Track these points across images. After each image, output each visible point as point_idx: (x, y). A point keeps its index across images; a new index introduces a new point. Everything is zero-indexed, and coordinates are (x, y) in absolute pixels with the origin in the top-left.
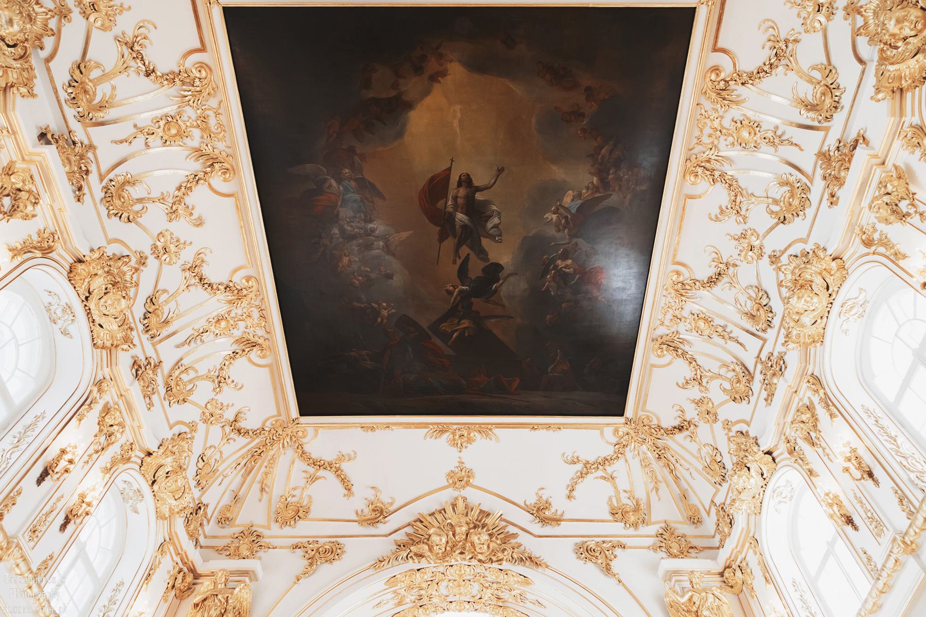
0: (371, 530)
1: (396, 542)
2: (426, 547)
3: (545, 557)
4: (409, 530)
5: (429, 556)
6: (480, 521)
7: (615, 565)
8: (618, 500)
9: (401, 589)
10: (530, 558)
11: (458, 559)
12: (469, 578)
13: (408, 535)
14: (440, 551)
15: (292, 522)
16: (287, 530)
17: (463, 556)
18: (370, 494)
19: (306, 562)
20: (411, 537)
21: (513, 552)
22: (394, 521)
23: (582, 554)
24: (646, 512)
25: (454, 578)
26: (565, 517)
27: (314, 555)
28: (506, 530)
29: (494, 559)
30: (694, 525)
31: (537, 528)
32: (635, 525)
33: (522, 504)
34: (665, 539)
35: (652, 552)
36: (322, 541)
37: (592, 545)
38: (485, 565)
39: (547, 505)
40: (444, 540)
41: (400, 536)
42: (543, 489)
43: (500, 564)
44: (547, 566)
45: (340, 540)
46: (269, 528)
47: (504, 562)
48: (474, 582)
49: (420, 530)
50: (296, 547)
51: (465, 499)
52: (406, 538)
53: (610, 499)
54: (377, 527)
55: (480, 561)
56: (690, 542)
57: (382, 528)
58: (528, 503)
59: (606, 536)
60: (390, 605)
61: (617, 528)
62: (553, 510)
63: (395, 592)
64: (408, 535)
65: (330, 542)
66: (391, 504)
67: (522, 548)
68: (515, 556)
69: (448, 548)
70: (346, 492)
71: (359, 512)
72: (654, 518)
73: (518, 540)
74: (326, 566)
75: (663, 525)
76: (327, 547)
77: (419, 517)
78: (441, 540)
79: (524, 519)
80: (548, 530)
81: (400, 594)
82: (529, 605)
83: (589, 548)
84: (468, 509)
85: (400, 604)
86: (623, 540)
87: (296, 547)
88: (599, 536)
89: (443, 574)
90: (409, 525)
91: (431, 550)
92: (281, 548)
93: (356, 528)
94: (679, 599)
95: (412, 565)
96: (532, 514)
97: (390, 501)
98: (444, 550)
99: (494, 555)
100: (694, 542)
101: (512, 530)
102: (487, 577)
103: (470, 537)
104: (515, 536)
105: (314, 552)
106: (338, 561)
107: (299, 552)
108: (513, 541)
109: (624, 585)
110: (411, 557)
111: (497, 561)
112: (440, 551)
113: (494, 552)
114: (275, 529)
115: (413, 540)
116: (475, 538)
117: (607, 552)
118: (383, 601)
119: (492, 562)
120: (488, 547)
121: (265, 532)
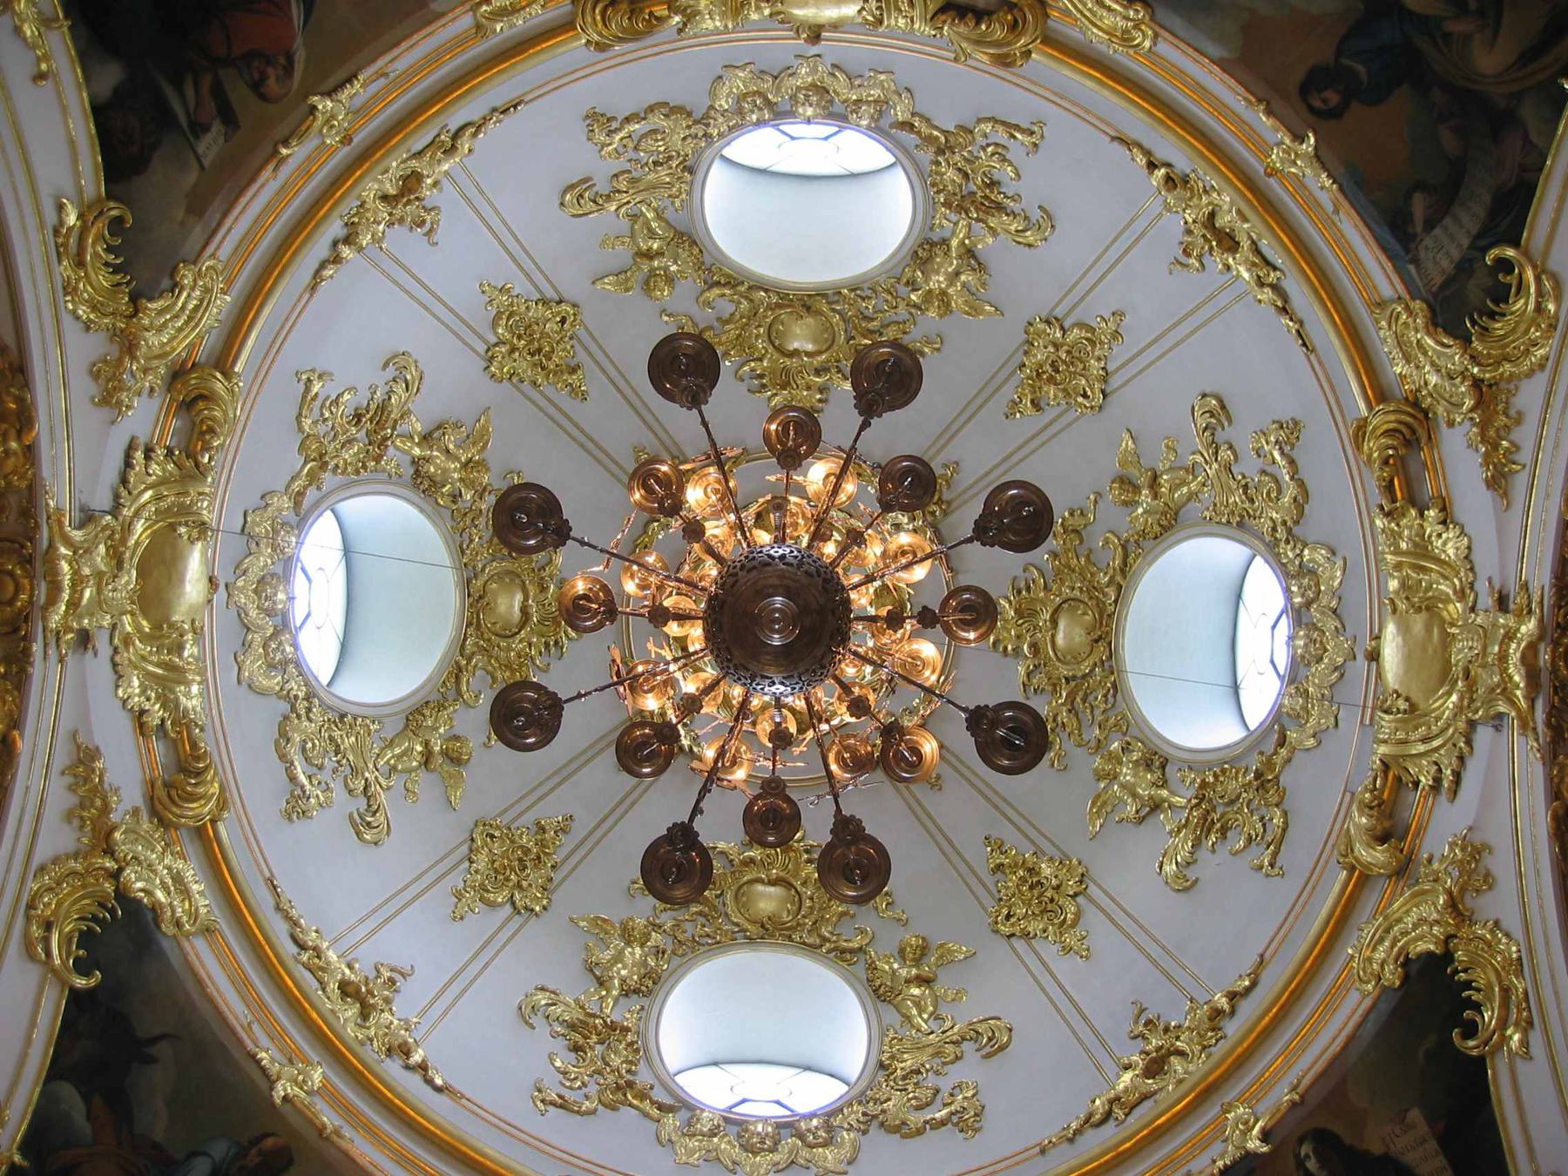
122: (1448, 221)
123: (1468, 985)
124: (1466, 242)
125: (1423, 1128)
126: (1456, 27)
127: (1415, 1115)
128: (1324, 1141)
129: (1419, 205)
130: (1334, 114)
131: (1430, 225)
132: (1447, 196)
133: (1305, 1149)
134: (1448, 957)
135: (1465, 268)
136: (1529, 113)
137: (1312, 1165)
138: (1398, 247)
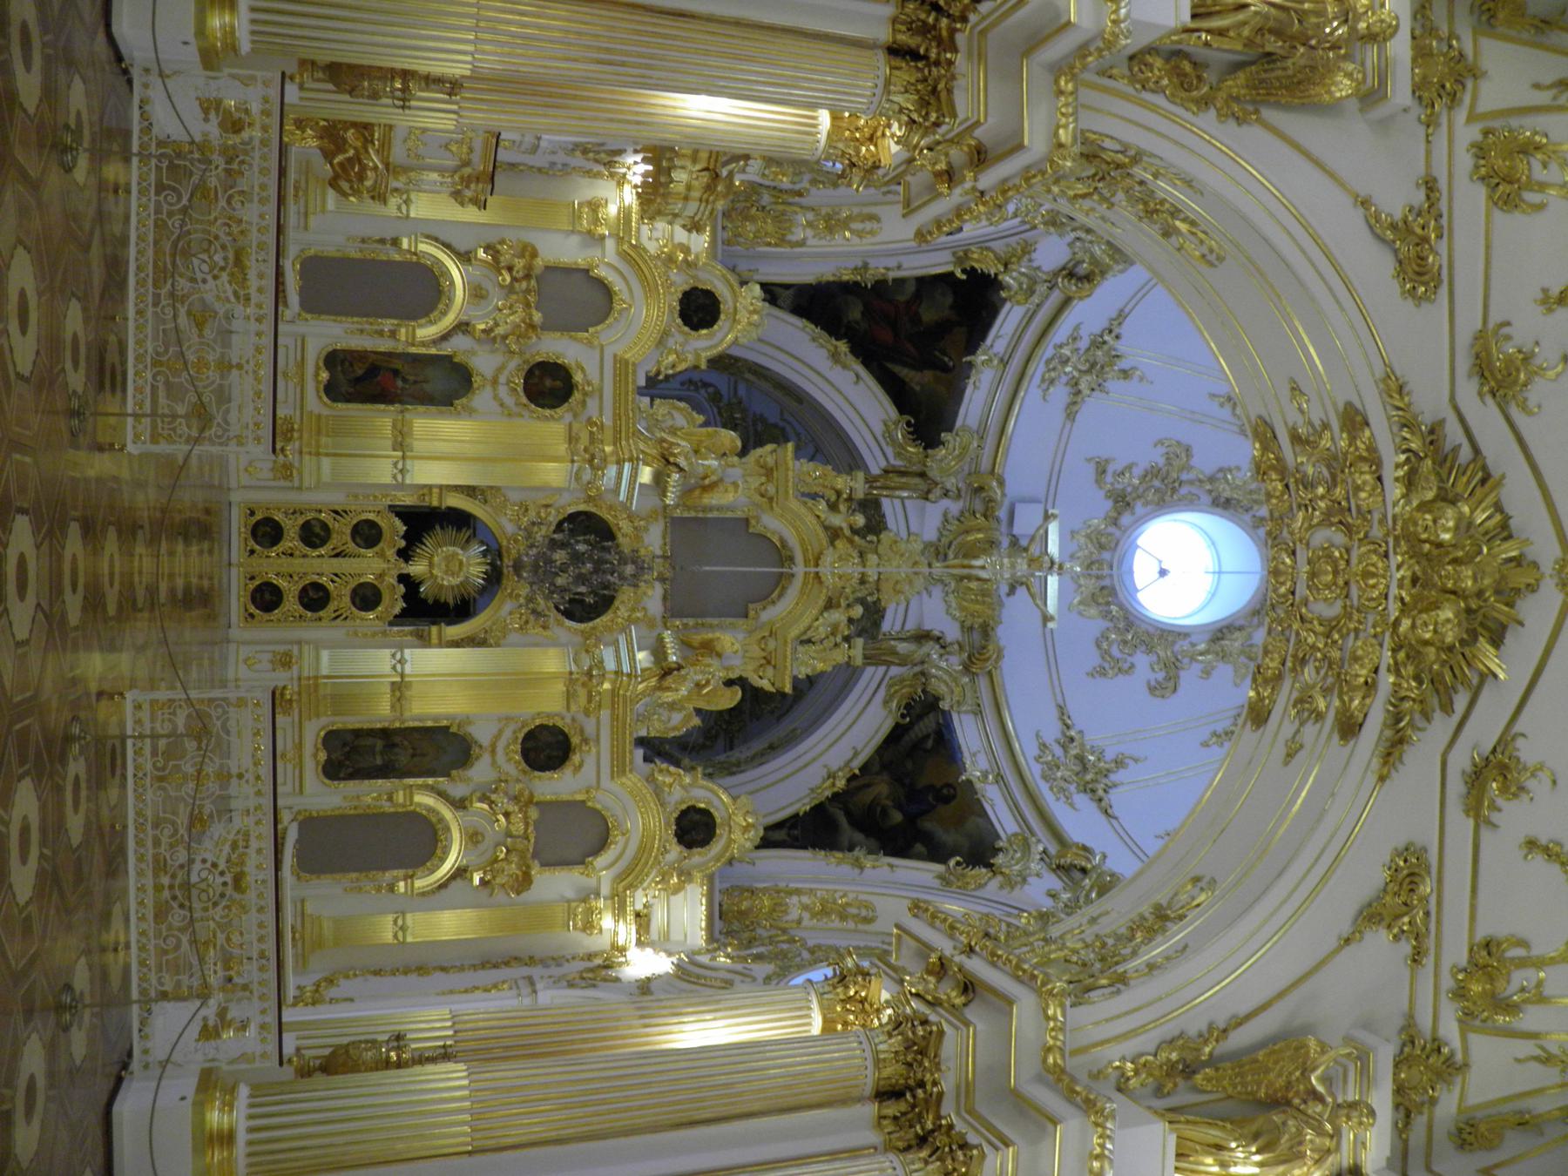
0: (1464, 364)
1: (1442, 422)
2: (1430, 495)
3: (1399, 778)
4: (1466, 453)
5: (1408, 502)
6: (1482, 624)
7: (1379, 939)
8: (1522, 963)
9: (1333, 439)
10: (1401, 741)
11: (1402, 572)
12: (1354, 592)
13: (1456, 449)
14: (1420, 529)
15: (1483, 171)
16: (1465, 161)
17: (1407, 582)
18: (1547, 355)
19: (1398, 216)
20: (1450, 457)
21: (1414, 700)
22: (1486, 419)
23: (1406, 861)
24: (1490, 1023)
25: (1354, 560)
26: (1486, 834)
27: (1413, 233)
28: (1460, 687)
29: (1401, 655)
30: (1453, 1130)
31: (1461, 760)
32: (1460, 993)
33: (1519, 727)
34: (1428, 1057)
35: (1399, 1022)
36: (1443, 247)
37: (1427, 888)
38: (1388, 635)
39: (1513, 789)
40: (1446, 536)
41: (1454, 434)
42: (1554, 782)
43: (1389, 670)
44: (1382, 779)
45: (1444, 291)
46: (1472, 118)
47: (1391, 679)
48: (1345, 607)
49: (1465, 479)
50: (1430, 185)
51: (1532, 588)
52: (1448, 447)
53: (1523, 943)
54: (1470, 376)
55: (1397, 623)
56: (1421, 1113)
57: (1468, 391)
58: (1520, 742)
59: (1439, 922)
60: (1294, 417)
61: (1456, 951)
62: (1500, 802)
63: (1326, 426)
64: (1456, 449)
65: (1440, 266)
66: (1524, 407)
67: (1420, 723)
68: (1407, 705)
69: (1427, 546)
70: (1555, 291)
71: (1506, 330)
72: (1475, 1039)
73: (1438, 715)
74: (1388, 264)
75: (1459, 1057)
76: (1431, 259)
77: (1496, 473)
78: (1447, 530)
79: (1484, 730)
80: (1456, 786)
81: (1320, 437)
82: (1288, 730)
83: (1416, 879)
84: (1509, 595)
85: (1296, 438)
86: (1429, 962)
87: (1430, 185)
88: (1439, 903)
89: (1366, 536)
90: (1476, 450)
91: (1424, 507)
92: (1428, 153)
93: (1469, 322)
94: (1319, 1072)
95: (1393, 461)
96: (1494, 751)
97: (1532, 403)
98: (1424, 536)
99: (1408, 657)
100: (1419, 1122)
101: (1461, 701)
102: (1357, 638)
103: (1448, 600)
104: (1447, 708)
105: (1419, 231)
106: (1399, 290)
107: (1419, 197)
108: (1435, 701)
109: (1340, 948)
110: (1408, 460)
111: (1396, 663)
112: (1420, 529)
113: (1415, 655)
114: (1468, 134)
115: (1444, 460)
116: (1447, 613)
117: (1406, 919)
118: (1308, 401)
119: (1394, 651)
120: (1426, 643)
121: (1461, 115)
122: (920, 735)
123: (914, 440)
124: (916, 728)
125: (913, 385)
126: (889, 803)
127: (918, 388)
128: (945, 369)
129: (930, 744)
130: (949, 785)
131: (928, 736)
132: (917, 746)
133: (951, 364)
134: (925, 448)
135: (920, 717)
136: (876, 768)
137: (946, 359)
138: (944, 730)
